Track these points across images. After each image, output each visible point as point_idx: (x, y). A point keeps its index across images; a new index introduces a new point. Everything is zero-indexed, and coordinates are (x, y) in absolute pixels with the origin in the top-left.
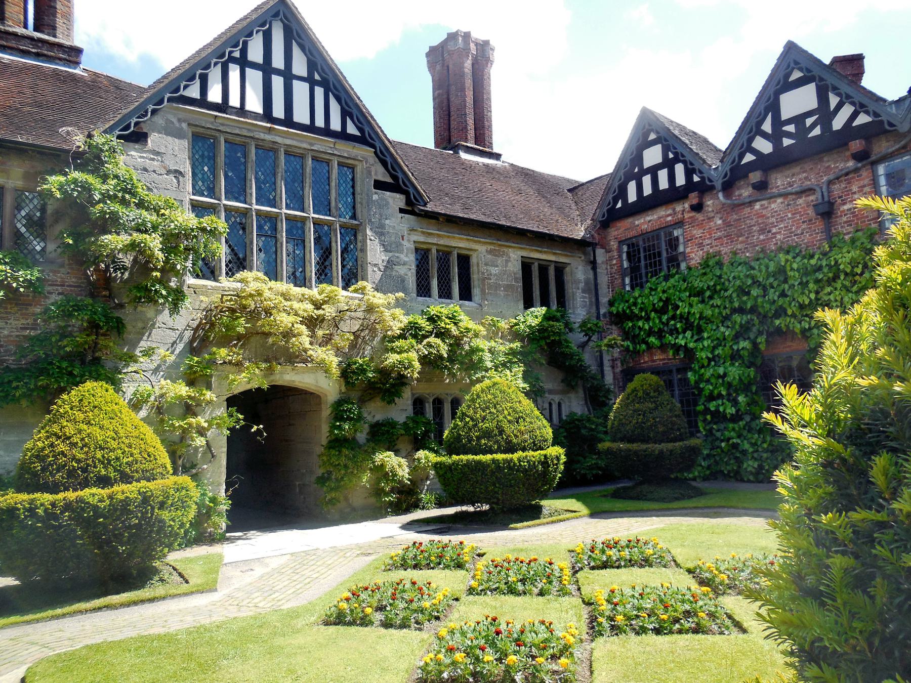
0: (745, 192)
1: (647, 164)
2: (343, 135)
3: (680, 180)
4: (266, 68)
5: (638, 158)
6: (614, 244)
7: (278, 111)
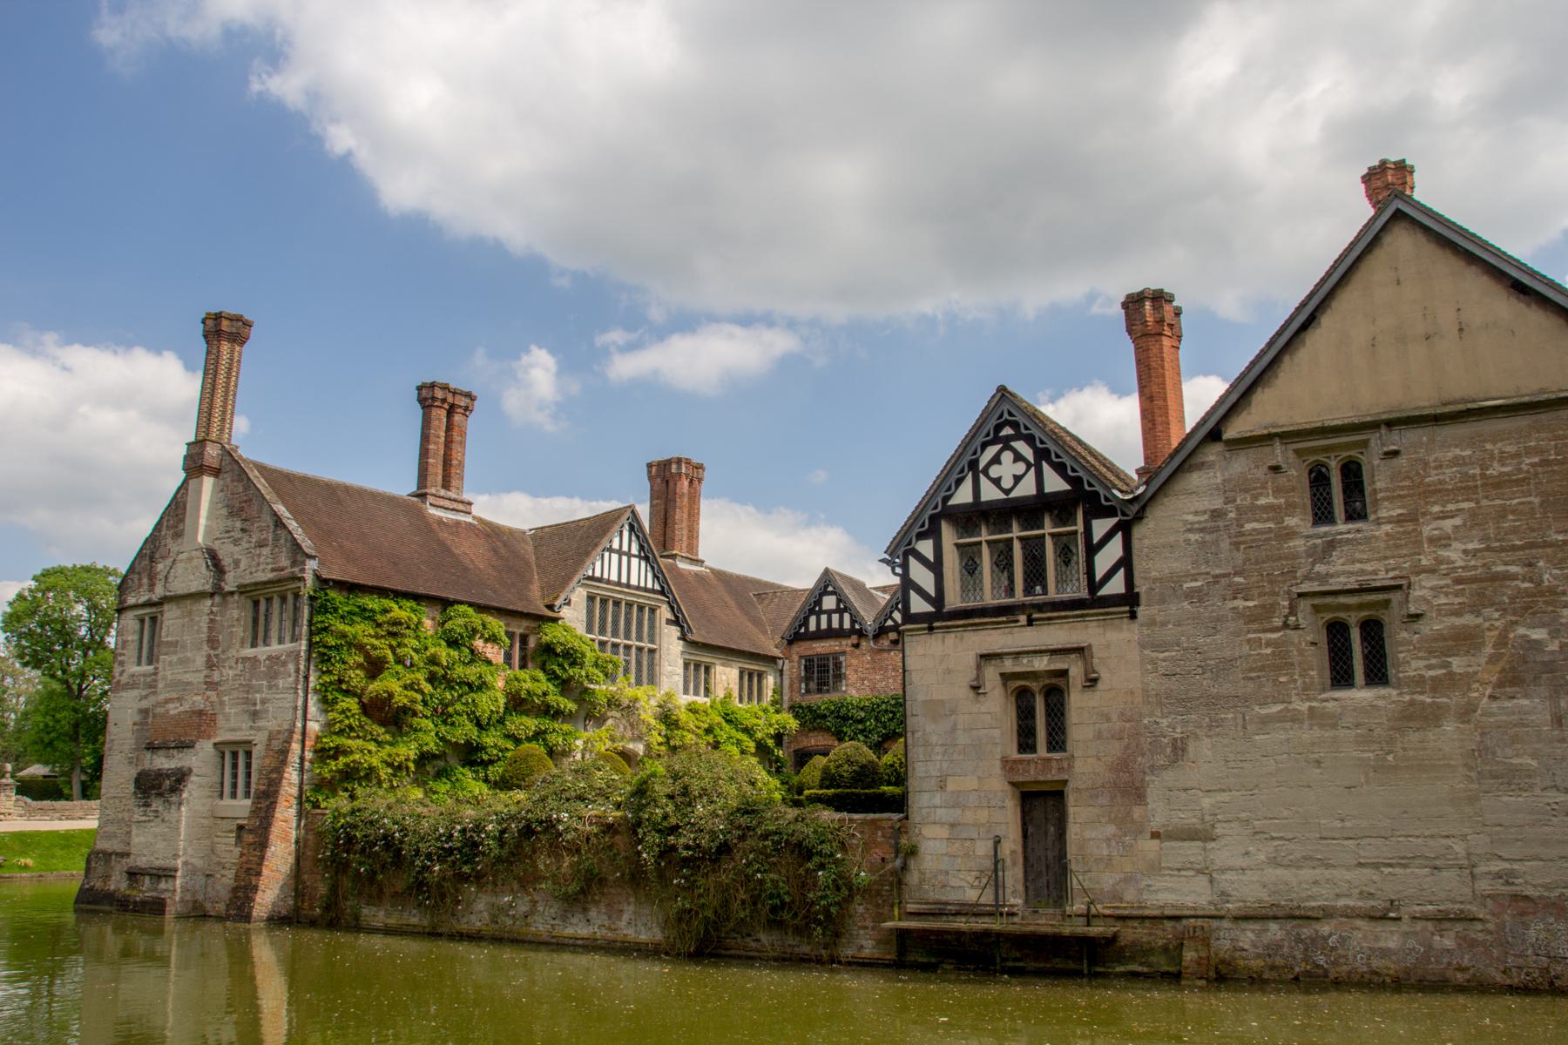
0: (885, 643)
1: (825, 607)
2: (653, 591)
3: (847, 625)
4: (620, 552)
5: (819, 602)
6: (795, 657)
7: (624, 580)
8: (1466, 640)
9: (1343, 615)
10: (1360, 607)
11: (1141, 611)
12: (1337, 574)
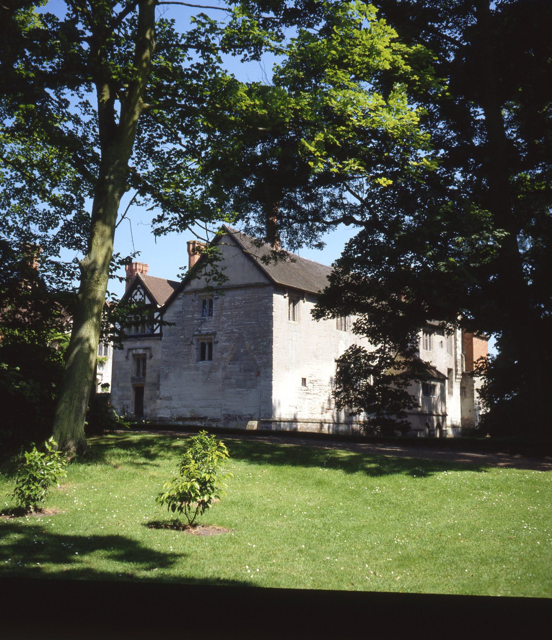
8: (225, 349)
9: (204, 341)
10: (208, 339)
11: (163, 338)
12: (203, 330)
